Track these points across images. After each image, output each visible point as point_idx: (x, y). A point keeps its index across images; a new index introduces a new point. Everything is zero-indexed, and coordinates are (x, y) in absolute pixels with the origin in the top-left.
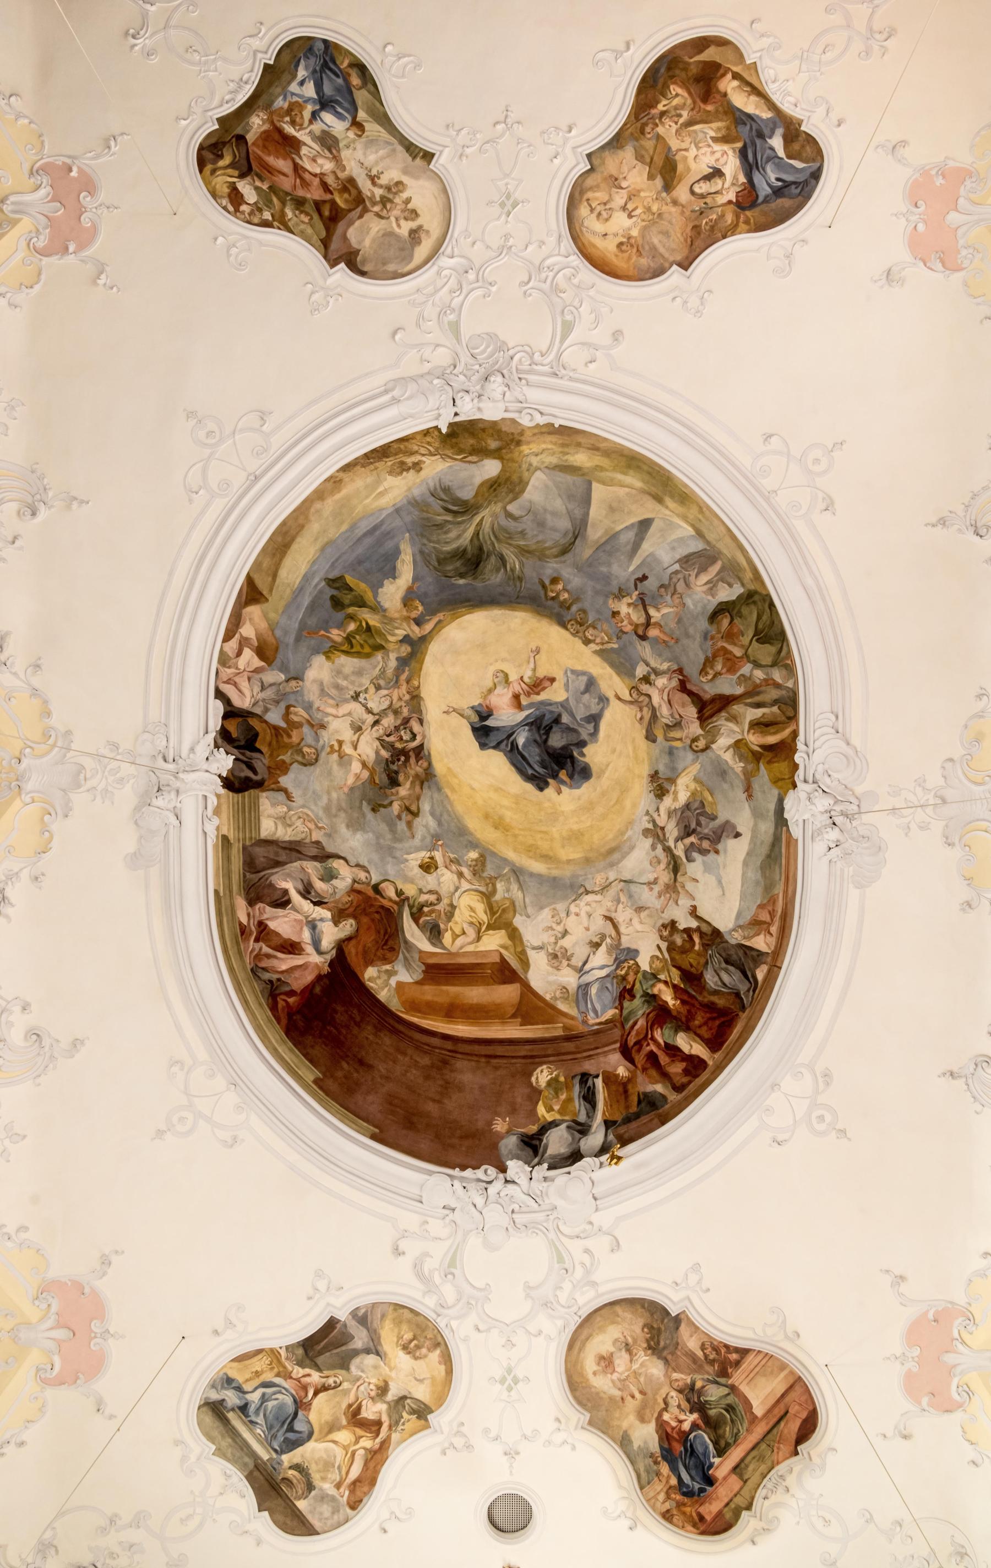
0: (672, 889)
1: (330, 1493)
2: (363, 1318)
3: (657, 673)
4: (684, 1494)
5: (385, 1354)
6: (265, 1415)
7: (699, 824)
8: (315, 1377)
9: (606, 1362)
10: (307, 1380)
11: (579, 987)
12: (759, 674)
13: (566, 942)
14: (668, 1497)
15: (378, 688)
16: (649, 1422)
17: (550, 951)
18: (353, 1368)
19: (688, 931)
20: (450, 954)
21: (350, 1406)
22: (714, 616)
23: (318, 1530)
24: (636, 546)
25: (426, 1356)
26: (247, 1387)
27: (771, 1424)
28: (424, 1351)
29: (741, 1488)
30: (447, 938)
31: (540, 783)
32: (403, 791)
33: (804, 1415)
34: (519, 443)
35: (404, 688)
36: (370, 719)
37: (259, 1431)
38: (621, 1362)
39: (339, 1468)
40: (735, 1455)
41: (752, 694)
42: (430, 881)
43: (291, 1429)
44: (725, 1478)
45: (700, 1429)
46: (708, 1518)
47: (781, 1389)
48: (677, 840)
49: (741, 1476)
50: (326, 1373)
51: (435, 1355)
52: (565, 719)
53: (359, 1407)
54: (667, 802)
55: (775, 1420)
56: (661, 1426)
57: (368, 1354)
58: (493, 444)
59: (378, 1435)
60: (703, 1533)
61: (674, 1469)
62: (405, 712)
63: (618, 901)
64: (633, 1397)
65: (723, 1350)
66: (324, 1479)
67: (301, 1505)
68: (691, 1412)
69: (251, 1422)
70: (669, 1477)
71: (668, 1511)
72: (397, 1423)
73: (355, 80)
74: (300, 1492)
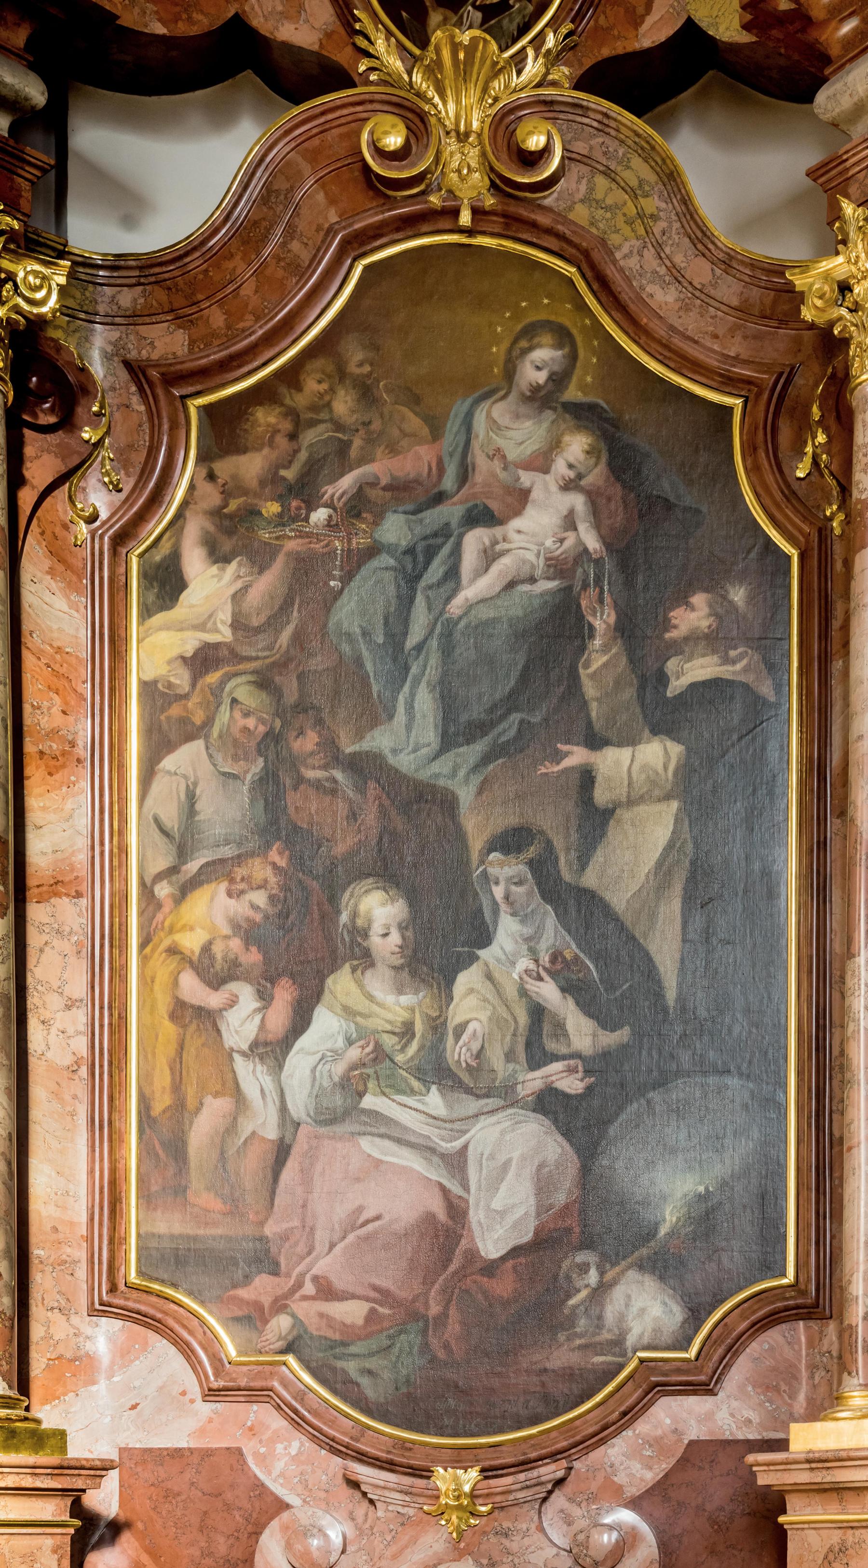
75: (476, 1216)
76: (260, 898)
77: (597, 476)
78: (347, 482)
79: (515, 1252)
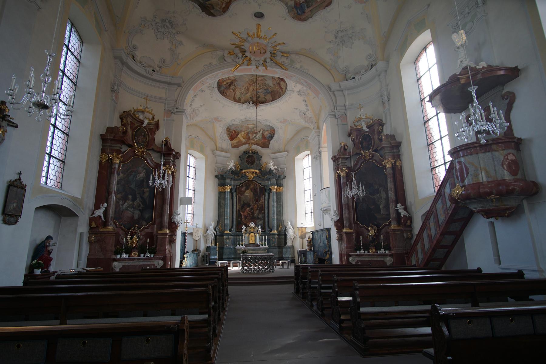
39: (220, 5)
40: (311, 8)
44: (307, 12)
46: (302, 18)
67: (212, 11)
70: (295, 11)
75: (134, 217)
76: (123, 195)
77: (145, 173)
78: (130, 170)
79: (137, 219)
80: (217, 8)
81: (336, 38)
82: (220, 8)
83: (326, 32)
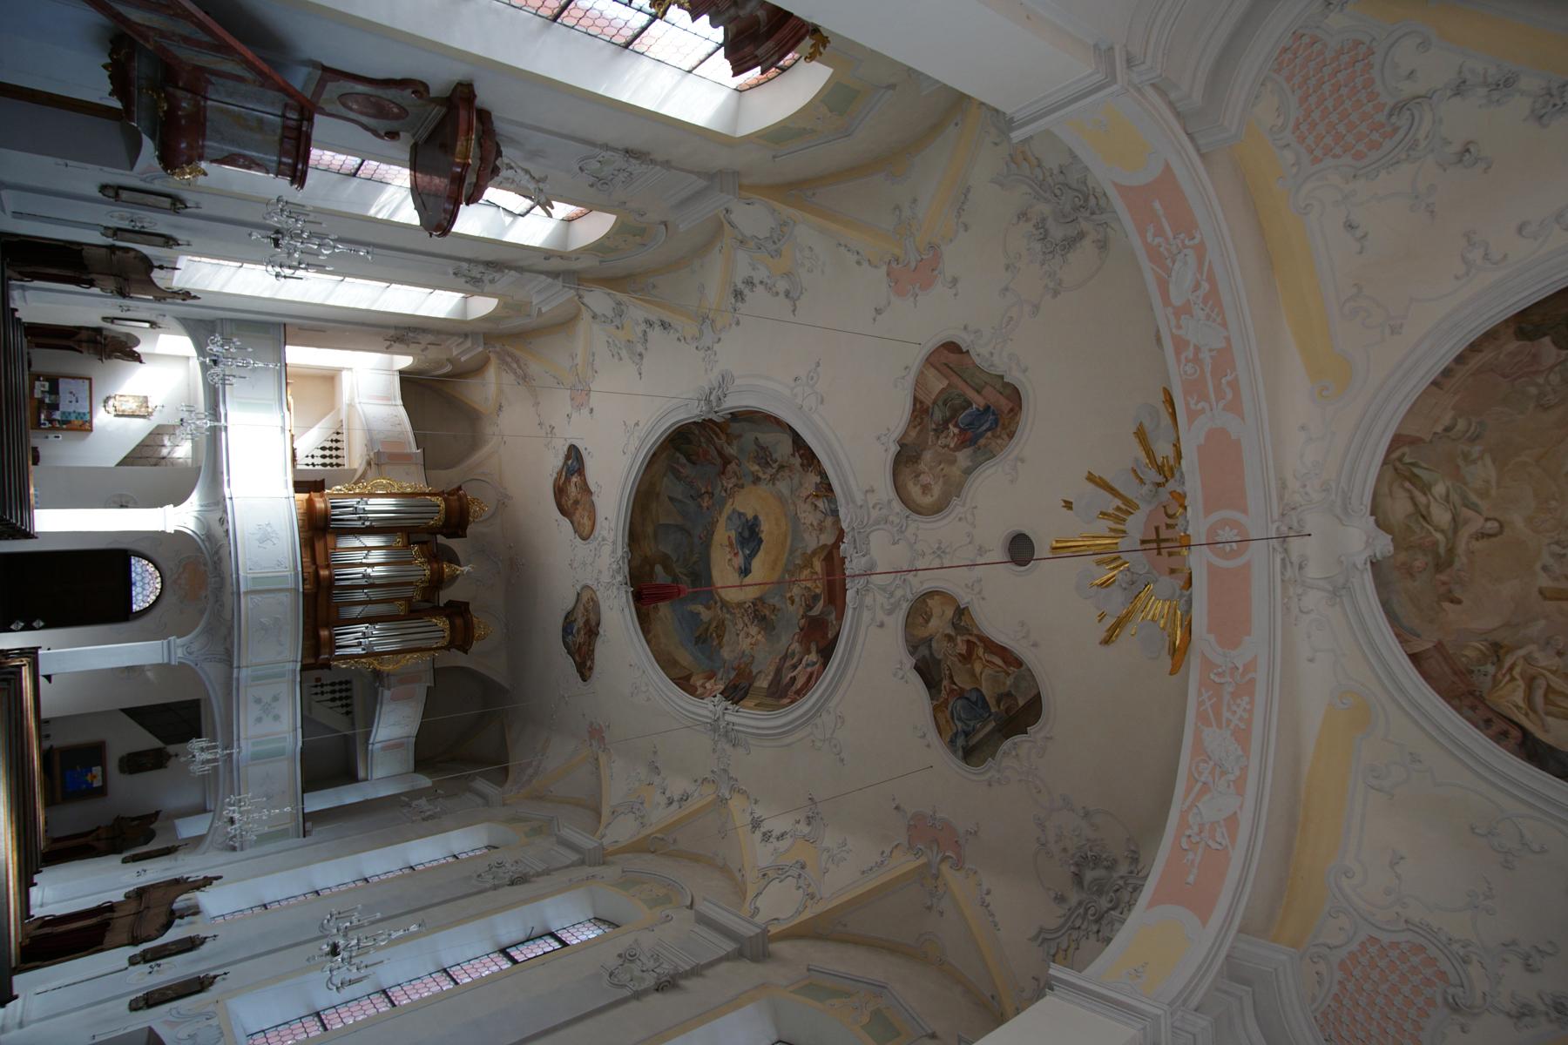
0: (790, 468)
1: (1012, 680)
2: (913, 648)
3: (723, 486)
4: (997, 426)
5: (931, 635)
6: (970, 720)
7: (762, 458)
8: (945, 683)
9: (926, 489)
10: (947, 688)
11: (832, 515)
12: (702, 440)
13: (815, 524)
14: (999, 437)
15: (736, 624)
16: (955, 456)
17: (818, 532)
18: (939, 657)
19: (801, 457)
20: (824, 589)
21: (960, 661)
22: (694, 463)
23: (1036, 692)
24: (680, 501)
25: (931, 609)
26: (955, 731)
27: (952, 373)
28: (928, 609)
29: (991, 385)
30: (818, 591)
31: (761, 541)
32: (767, 613)
33: (946, 352)
34: (646, 557)
35: (736, 611)
36: (745, 628)
37: (978, 725)
38: (925, 479)
39: (997, 672)
40: (971, 394)
41: (710, 441)
42: (797, 599)
43: (975, 703)
44: (985, 398)
45: (956, 422)
46: (1011, 405)
47: (932, 370)
48: (773, 468)
49: (983, 387)
50: (943, 675)
51: (929, 602)
52: (740, 530)
53: (960, 654)
54: (760, 474)
55: (949, 371)
56: (957, 448)
57: (931, 647)
58: (648, 568)
59: (974, 643)
60: (1021, 408)
61: (981, 435)
62: (743, 610)
63: (799, 496)
64: (942, 469)
65: (915, 413)
66: (1004, 684)
67: (1021, 703)
68: (948, 429)
69: (974, 730)
71: (1008, 435)
72: (968, 630)
73: (568, 620)
74: (1013, 702)
80: (1008, 683)
81: (1082, 235)
82: (1008, 674)
83: (1056, 293)
